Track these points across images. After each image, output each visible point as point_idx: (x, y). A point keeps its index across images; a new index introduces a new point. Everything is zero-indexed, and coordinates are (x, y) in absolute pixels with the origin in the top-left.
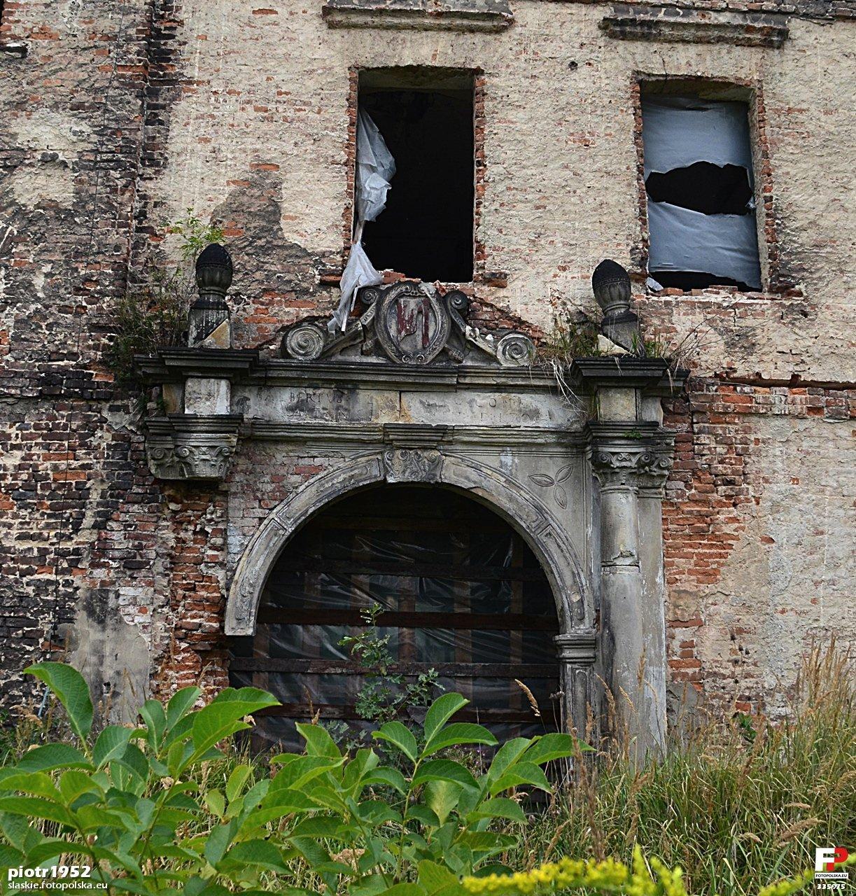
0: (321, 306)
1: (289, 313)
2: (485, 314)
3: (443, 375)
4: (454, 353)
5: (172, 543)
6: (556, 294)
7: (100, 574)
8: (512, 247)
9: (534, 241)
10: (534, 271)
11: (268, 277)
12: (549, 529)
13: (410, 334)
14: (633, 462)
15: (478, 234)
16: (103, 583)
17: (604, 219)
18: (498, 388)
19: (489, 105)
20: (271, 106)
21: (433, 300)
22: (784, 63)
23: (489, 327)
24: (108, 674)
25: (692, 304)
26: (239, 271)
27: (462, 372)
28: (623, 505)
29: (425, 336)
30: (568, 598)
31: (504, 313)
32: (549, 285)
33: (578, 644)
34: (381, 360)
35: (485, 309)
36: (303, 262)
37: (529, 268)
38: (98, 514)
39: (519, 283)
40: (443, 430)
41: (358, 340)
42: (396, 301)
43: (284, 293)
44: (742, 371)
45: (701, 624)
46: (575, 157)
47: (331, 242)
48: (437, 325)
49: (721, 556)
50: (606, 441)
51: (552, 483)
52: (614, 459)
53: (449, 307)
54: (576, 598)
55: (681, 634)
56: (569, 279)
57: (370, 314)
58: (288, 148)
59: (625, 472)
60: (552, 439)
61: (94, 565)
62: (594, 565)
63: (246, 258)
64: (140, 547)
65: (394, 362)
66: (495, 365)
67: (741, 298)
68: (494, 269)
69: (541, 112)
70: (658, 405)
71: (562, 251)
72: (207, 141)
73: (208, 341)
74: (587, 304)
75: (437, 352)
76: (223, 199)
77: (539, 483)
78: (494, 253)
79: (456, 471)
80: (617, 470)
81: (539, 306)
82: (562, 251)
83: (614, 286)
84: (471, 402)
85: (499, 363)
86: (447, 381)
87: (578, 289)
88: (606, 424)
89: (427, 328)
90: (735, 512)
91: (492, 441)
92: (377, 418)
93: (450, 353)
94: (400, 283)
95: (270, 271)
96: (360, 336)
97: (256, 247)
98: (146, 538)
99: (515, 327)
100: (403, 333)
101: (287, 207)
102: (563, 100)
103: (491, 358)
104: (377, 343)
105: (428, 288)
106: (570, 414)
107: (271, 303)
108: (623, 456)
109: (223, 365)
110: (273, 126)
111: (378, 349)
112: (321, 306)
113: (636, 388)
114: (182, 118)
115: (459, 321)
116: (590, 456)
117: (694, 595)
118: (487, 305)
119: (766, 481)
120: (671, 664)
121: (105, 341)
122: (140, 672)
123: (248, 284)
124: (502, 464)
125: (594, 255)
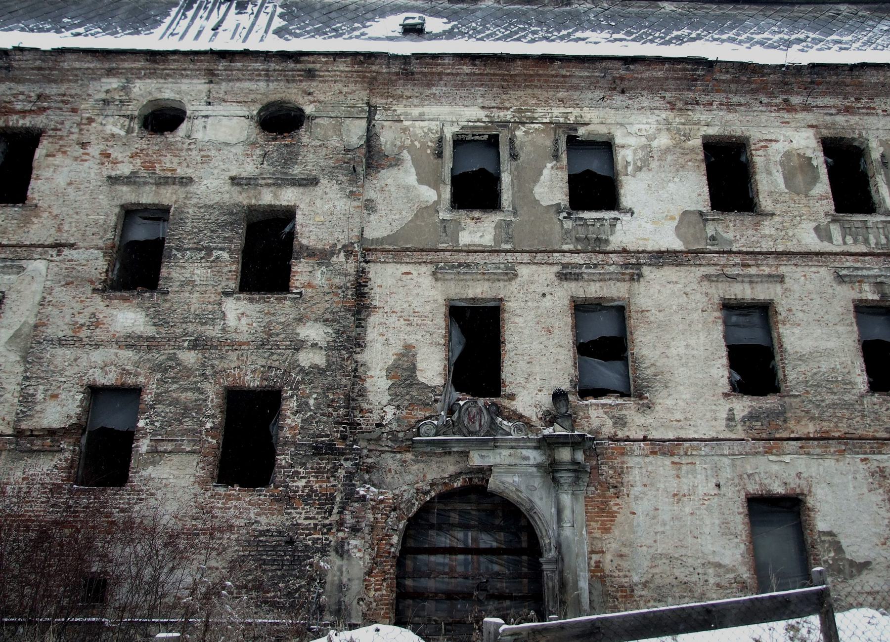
1: (420, 414)
5: (372, 520)
7: (341, 534)
11: (412, 398)
13: (473, 423)
15: (503, 376)
16: (342, 538)
17: (558, 367)
19: (506, 315)
20: (411, 318)
21: (483, 409)
22: (640, 288)
23: (509, 419)
24: (345, 580)
25: (597, 405)
28: (566, 499)
30: (545, 541)
33: (549, 562)
38: (340, 507)
39: (521, 398)
43: (418, 405)
44: (620, 435)
45: (603, 552)
46: (544, 339)
48: (485, 418)
49: (612, 521)
54: (547, 541)
55: (595, 557)
57: (456, 415)
58: (419, 338)
60: (535, 469)
61: (338, 531)
62: (555, 526)
64: (358, 522)
67: (620, 401)
69: (529, 318)
70: (582, 453)
71: (539, 383)
72: (383, 335)
76: (391, 362)
81: (530, 408)
82: (539, 383)
84: (500, 454)
87: (546, 400)
90: (618, 501)
98: (361, 517)
101: (420, 366)
102: (540, 311)
105: (481, 401)
106: (543, 458)
107: (413, 410)
110: (412, 328)
114: (372, 325)
117: (600, 539)
119: (632, 486)
120: (590, 571)
121: (341, 429)
122: (359, 579)
124: (514, 481)
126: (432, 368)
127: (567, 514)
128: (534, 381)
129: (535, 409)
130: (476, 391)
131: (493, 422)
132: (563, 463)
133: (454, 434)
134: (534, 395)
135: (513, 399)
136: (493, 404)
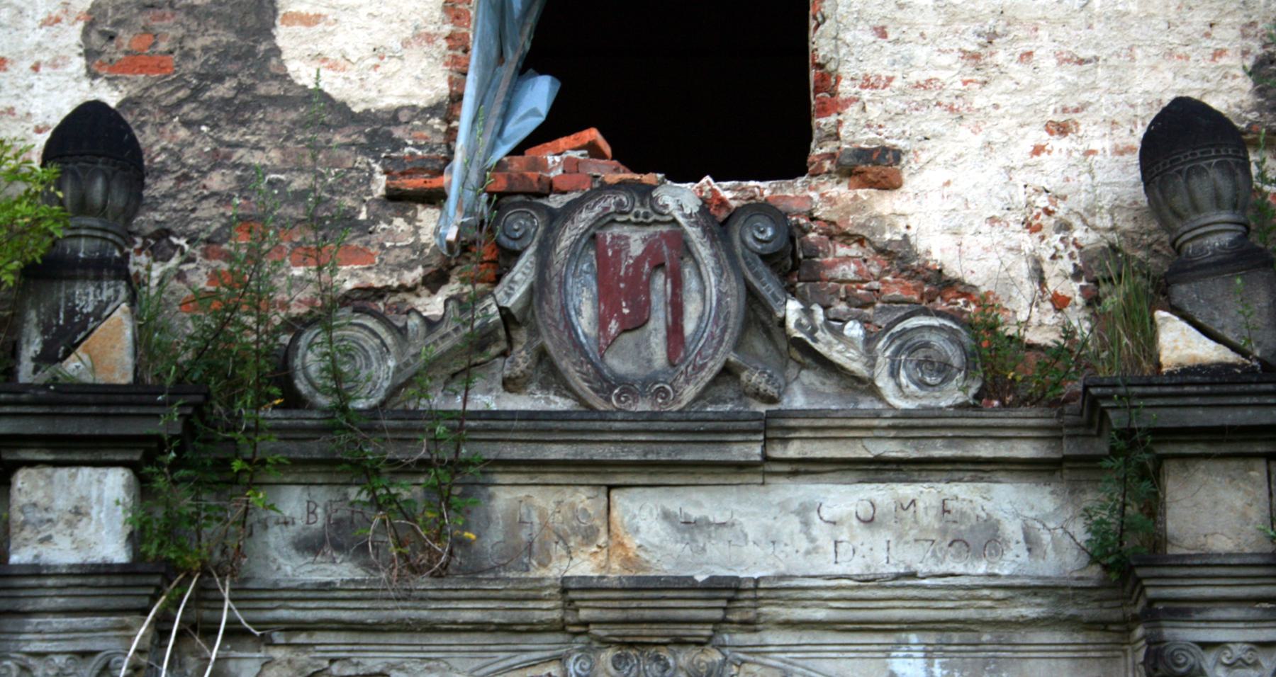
0: (390, 259)
2: (844, 263)
3: (727, 437)
4: (754, 378)
6: (1042, 201)
8: (915, 76)
10: (978, 140)
13: (637, 323)
18: (878, 469)
21: (694, 233)
26: (163, 171)
27: (774, 427)
29: (675, 330)
31: (899, 257)
32: (1020, 178)
34: (561, 404)
35: (842, 251)
36: (338, 139)
37: (963, 132)
40: (727, 590)
41: (494, 350)
47: (413, 81)
48: (706, 293)
53: (739, 249)
57: (522, 275)
63: (183, 133)
65: (591, 409)
66: (866, 404)
68: (865, 138)
71: (1053, 81)
73: (75, 366)
74: (1129, 226)
75: (706, 376)
78: (866, 94)
83: (1200, 172)
84: (804, 513)
85: (881, 399)
88: (1181, 561)
89: (677, 309)
92: (543, 564)
93: (744, 376)
94: (605, 188)
95: (247, 167)
96: (497, 340)
97: (209, 104)
100: (613, 326)
104: (542, 355)
105: (680, 199)
109: (113, 428)
111: (547, 372)
112: (390, 259)
118: (847, 238)
123: (189, 204)
125: (1148, 86)
128: (1021, 73)
129: (1028, 242)
131: (758, 316)
133: (511, 385)
134: (1020, 152)
135: (889, 184)
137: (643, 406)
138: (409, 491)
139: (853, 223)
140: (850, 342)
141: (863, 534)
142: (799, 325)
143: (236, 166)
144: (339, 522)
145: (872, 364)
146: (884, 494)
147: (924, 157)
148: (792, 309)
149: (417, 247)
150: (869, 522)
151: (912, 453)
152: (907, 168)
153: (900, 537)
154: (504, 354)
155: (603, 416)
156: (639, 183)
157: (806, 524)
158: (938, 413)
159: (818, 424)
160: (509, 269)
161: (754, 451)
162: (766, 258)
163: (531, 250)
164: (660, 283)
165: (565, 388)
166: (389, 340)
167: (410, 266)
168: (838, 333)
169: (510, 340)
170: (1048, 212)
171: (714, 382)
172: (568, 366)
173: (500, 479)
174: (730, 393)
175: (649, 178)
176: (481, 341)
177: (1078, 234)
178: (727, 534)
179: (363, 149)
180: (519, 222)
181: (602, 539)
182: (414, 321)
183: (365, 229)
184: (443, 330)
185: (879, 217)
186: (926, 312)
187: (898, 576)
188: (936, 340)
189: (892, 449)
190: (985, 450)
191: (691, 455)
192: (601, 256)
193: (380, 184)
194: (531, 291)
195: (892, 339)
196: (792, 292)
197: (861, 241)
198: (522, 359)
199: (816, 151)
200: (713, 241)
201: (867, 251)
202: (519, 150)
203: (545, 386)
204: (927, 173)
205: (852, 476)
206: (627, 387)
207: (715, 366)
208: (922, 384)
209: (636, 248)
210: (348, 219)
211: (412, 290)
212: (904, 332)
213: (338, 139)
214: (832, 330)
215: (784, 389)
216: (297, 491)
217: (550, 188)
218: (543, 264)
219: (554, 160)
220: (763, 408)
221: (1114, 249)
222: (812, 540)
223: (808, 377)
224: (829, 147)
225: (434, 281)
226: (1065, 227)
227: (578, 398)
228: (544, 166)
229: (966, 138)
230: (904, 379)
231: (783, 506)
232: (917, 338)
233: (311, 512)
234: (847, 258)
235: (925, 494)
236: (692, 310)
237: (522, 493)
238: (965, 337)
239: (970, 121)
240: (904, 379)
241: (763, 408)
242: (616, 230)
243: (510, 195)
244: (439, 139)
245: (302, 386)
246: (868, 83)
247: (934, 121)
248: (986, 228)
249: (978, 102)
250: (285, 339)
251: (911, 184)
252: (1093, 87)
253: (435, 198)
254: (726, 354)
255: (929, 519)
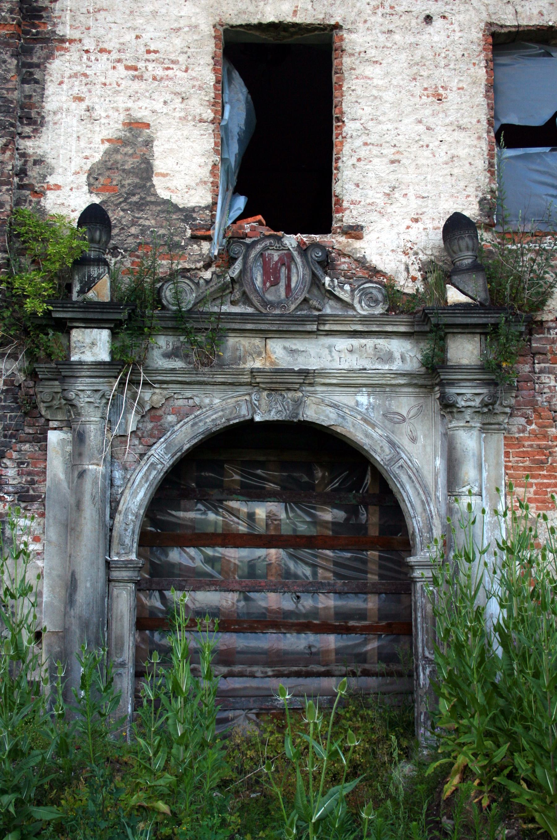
0: (192, 259)
2: (344, 264)
3: (304, 322)
4: (314, 303)
6: (409, 245)
8: (368, 201)
9: (389, 195)
10: (389, 223)
11: (143, 232)
12: (401, 462)
13: (275, 283)
14: (477, 402)
15: (337, 188)
17: (455, 171)
19: (347, 61)
20: (141, 65)
21: (295, 254)
26: (115, 226)
27: (321, 319)
28: (469, 441)
29: (288, 286)
30: (416, 523)
31: (362, 262)
32: (402, 237)
34: (250, 310)
35: (343, 260)
36: (174, 217)
37: (384, 220)
40: (305, 373)
41: (228, 291)
42: (261, 255)
46: (428, 112)
47: (200, 198)
48: (299, 274)
50: (452, 383)
51: (404, 420)
52: (459, 399)
56: (421, 230)
57: (238, 266)
58: (158, 106)
59: (469, 411)
62: (441, 493)
63: (122, 213)
65: (261, 312)
66: (351, 313)
69: (396, 68)
71: (414, 204)
72: (80, 99)
73: (91, 295)
74: (437, 254)
75: (298, 302)
76: (97, 157)
77: (391, 420)
78: (352, 207)
79: (318, 410)
80: (463, 409)
81: (392, 256)
83: (462, 238)
86: (309, 328)
88: (452, 367)
91: (350, 382)
92: (244, 363)
93: (311, 302)
95: (144, 226)
97: (130, 203)
99: (371, 276)
100: (268, 284)
101: (159, 165)
102: (418, 53)
103: (349, 306)
104: (244, 293)
105: (291, 241)
108: (468, 396)
109: (105, 317)
110: (143, 85)
111: (246, 299)
113: (481, 334)
114: (56, 77)
115: (319, 272)
116: (438, 396)
118: (345, 255)
123: (124, 238)
125: (445, 207)
126: (188, 167)
127: (469, 472)
128: (403, 201)
129: (404, 259)
130: (282, 222)
131: (316, 282)
132: (460, 368)
133: (233, 303)
134: (402, 228)
135: (359, 237)
136: (316, 245)
137: (277, 312)
138: (200, 338)
139: (347, 250)
140: (346, 291)
141: (349, 355)
142: (329, 285)
143: (140, 225)
144: (177, 348)
145: (353, 300)
146: (356, 342)
147: (371, 229)
148: (327, 280)
149: (201, 255)
150: (351, 351)
151: (366, 330)
152: (365, 232)
153: (361, 356)
154: (231, 293)
155: (265, 315)
156: (276, 236)
157: (330, 351)
158: (373, 316)
159: (335, 318)
160: (233, 264)
161: (314, 328)
162: (318, 262)
163: (241, 258)
164: (283, 270)
165: (251, 304)
166: (193, 287)
167: (199, 261)
168: (342, 288)
169: (233, 288)
170: (411, 249)
171: (301, 304)
172: (253, 297)
173: (230, 335)
174: (306, 307)
175: (281, 233)
176: (223, 288)
177: (421, 256)
178: (304, 354)
179: (183, 221)
180: (236, 248)
181: (264, 355)
182: (202, 281)
183: (184, 248)
184: (211, 284)
185: (355, 249)
186: (371, 282)
187: (360, 370)
188: (374, 292)
189: (359, 328)
190: (389, 329)
191: (293, 329)
192: (264, 261)
193: (189, 233)
194: (241, 272)
195: (360, 291)
196: (326, 273)
197: (349, 256)
198: (237, 295)
199: (335, 225)
200: (301, 256)
201: (351, 260)
202: (234, 222)
203: (244, 304)
204: (371, 234)
205: (346, 336)
206: (273, 305)
207: (301, 298)
208: (369, 306)
209: (276, 258)
210: (177, 245)
211: (199, 269)
212: (364, 288)
213: (174, 217)
214: (339, 286)
215: (323, 307)
216: (163, 337)
217: (246, 236)
218: (245, 263)
219: (247, 226)
220: (317, 313)
221: (432, 261)
222: (332, 357)
223: (332, 302)
224: (339, 224)
225: (207, 266)
226: (416, 254)
227: (256, 309)
228: (243, 228)
229: (384, 223)
230: (363, 304)
231: (323, 345)
232: (368, 291)
233: (168, 344)
234: (345, 262)
235: (369, 342)
236: (294, 279)
237: (237, 339)
238: (383, 290)
239: (386, 217)
240: (363, 304)
241: (317, 313)
242: (269, 252)
243: (234, 239)
244: (209, 218)
245: (165, 302)
246: (353, 203)
247: (374, 216)
248: (390, 253)
249: (389, 210)
250: (158, 285)
251: (366, 238)
252: (427, 206)
253: (209, 238)
254: (305, 294)
255: (370, 351)
